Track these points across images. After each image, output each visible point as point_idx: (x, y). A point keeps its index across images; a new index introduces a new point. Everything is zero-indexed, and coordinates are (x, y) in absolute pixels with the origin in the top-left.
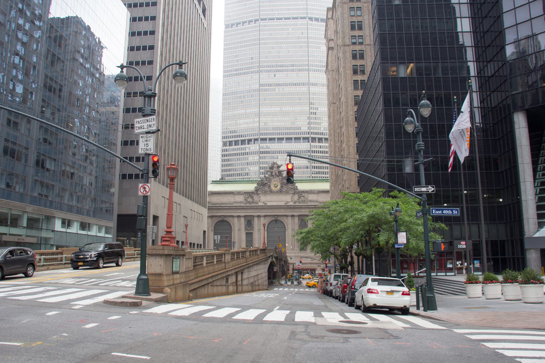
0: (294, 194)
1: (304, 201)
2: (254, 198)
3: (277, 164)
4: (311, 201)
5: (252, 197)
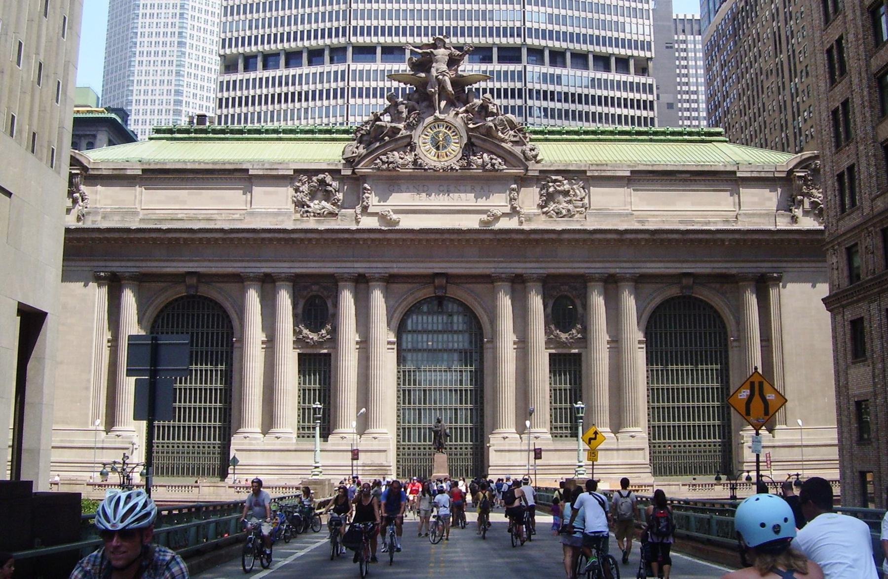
0: (524, 181)
4: (603, 213)
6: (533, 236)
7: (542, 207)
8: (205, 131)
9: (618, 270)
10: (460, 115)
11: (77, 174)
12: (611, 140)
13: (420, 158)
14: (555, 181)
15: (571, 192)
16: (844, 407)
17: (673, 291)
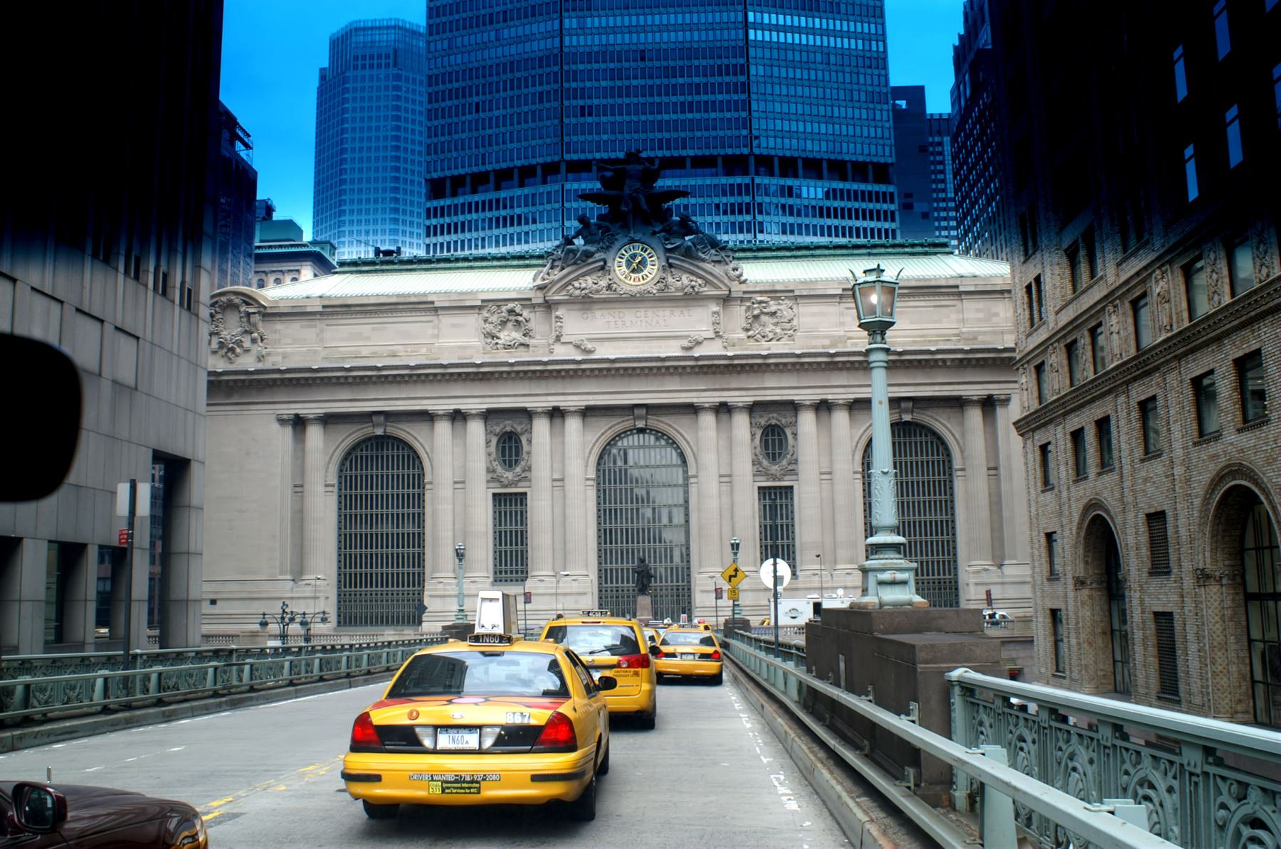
0: (726, 300)
2: (531, 325)
6: (736, 362)
7: (747, 330)
8: (392, 263)
9: (830, 397)
11: (254, 313)
12: (825, 256)
14: (761, 302)
16: (1035, 540)
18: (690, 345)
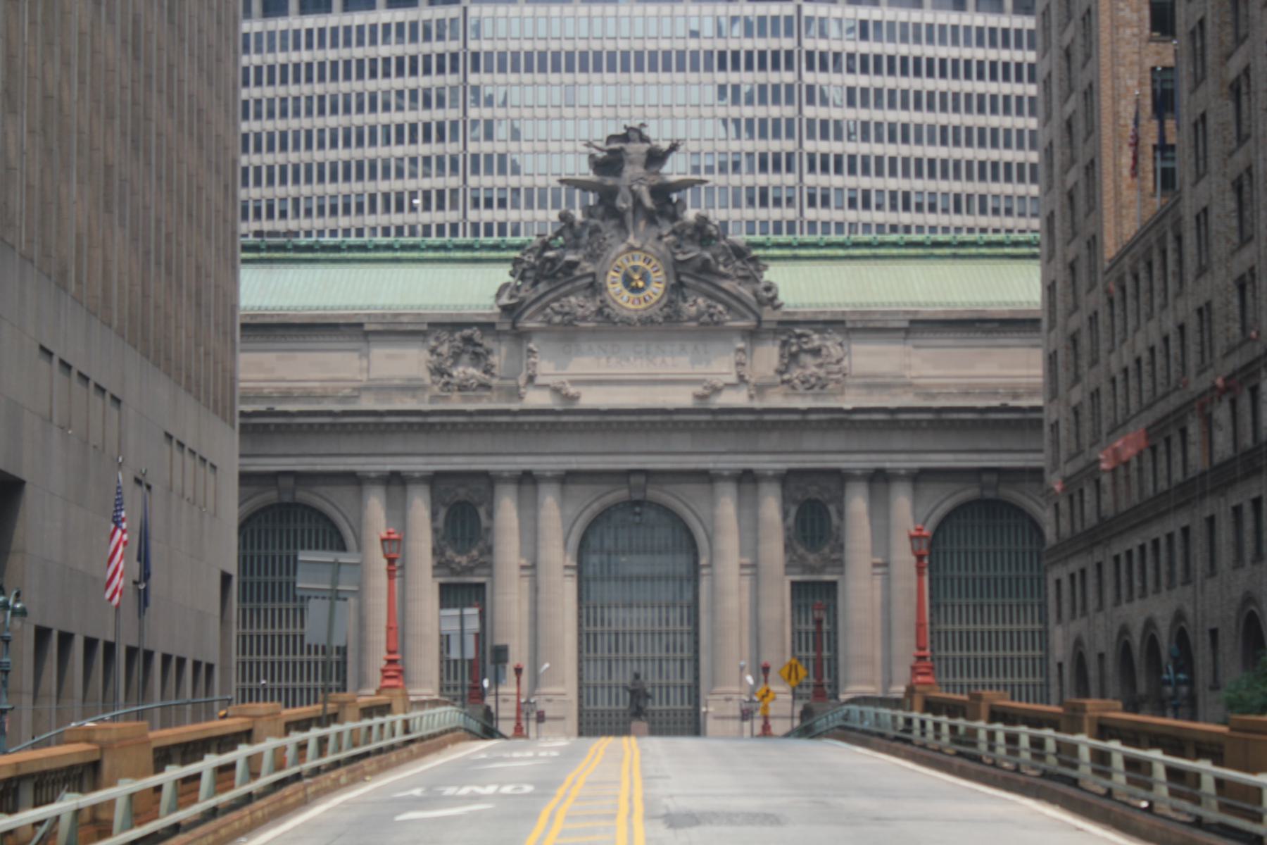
0: (754, 335)
1: (816, 385)
3: (644, 139)
5: (479, 357)
6: (768, 417)
7: (781, 373)
9: (888, 465)
10: (665, 240)
12: (893, 257)
13: (608, 306)
14: (800, 336)
15: (824, 352)
17: (970, 492)
18: (706, 392)
